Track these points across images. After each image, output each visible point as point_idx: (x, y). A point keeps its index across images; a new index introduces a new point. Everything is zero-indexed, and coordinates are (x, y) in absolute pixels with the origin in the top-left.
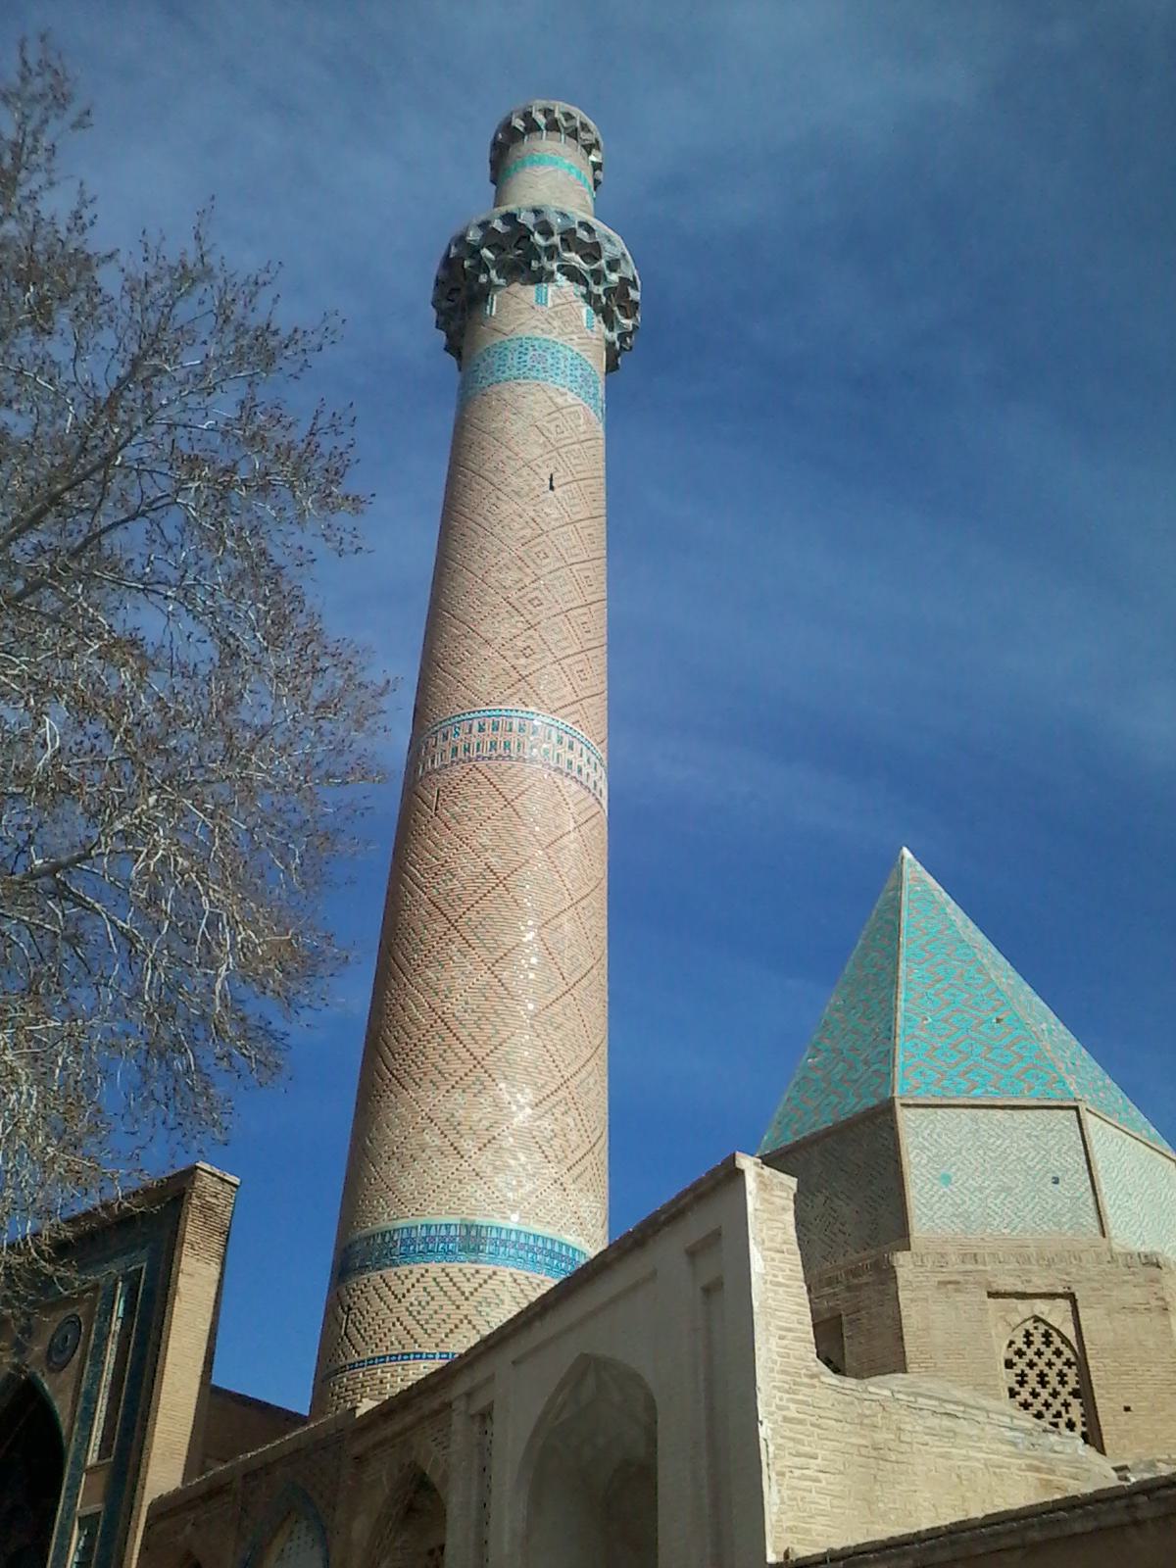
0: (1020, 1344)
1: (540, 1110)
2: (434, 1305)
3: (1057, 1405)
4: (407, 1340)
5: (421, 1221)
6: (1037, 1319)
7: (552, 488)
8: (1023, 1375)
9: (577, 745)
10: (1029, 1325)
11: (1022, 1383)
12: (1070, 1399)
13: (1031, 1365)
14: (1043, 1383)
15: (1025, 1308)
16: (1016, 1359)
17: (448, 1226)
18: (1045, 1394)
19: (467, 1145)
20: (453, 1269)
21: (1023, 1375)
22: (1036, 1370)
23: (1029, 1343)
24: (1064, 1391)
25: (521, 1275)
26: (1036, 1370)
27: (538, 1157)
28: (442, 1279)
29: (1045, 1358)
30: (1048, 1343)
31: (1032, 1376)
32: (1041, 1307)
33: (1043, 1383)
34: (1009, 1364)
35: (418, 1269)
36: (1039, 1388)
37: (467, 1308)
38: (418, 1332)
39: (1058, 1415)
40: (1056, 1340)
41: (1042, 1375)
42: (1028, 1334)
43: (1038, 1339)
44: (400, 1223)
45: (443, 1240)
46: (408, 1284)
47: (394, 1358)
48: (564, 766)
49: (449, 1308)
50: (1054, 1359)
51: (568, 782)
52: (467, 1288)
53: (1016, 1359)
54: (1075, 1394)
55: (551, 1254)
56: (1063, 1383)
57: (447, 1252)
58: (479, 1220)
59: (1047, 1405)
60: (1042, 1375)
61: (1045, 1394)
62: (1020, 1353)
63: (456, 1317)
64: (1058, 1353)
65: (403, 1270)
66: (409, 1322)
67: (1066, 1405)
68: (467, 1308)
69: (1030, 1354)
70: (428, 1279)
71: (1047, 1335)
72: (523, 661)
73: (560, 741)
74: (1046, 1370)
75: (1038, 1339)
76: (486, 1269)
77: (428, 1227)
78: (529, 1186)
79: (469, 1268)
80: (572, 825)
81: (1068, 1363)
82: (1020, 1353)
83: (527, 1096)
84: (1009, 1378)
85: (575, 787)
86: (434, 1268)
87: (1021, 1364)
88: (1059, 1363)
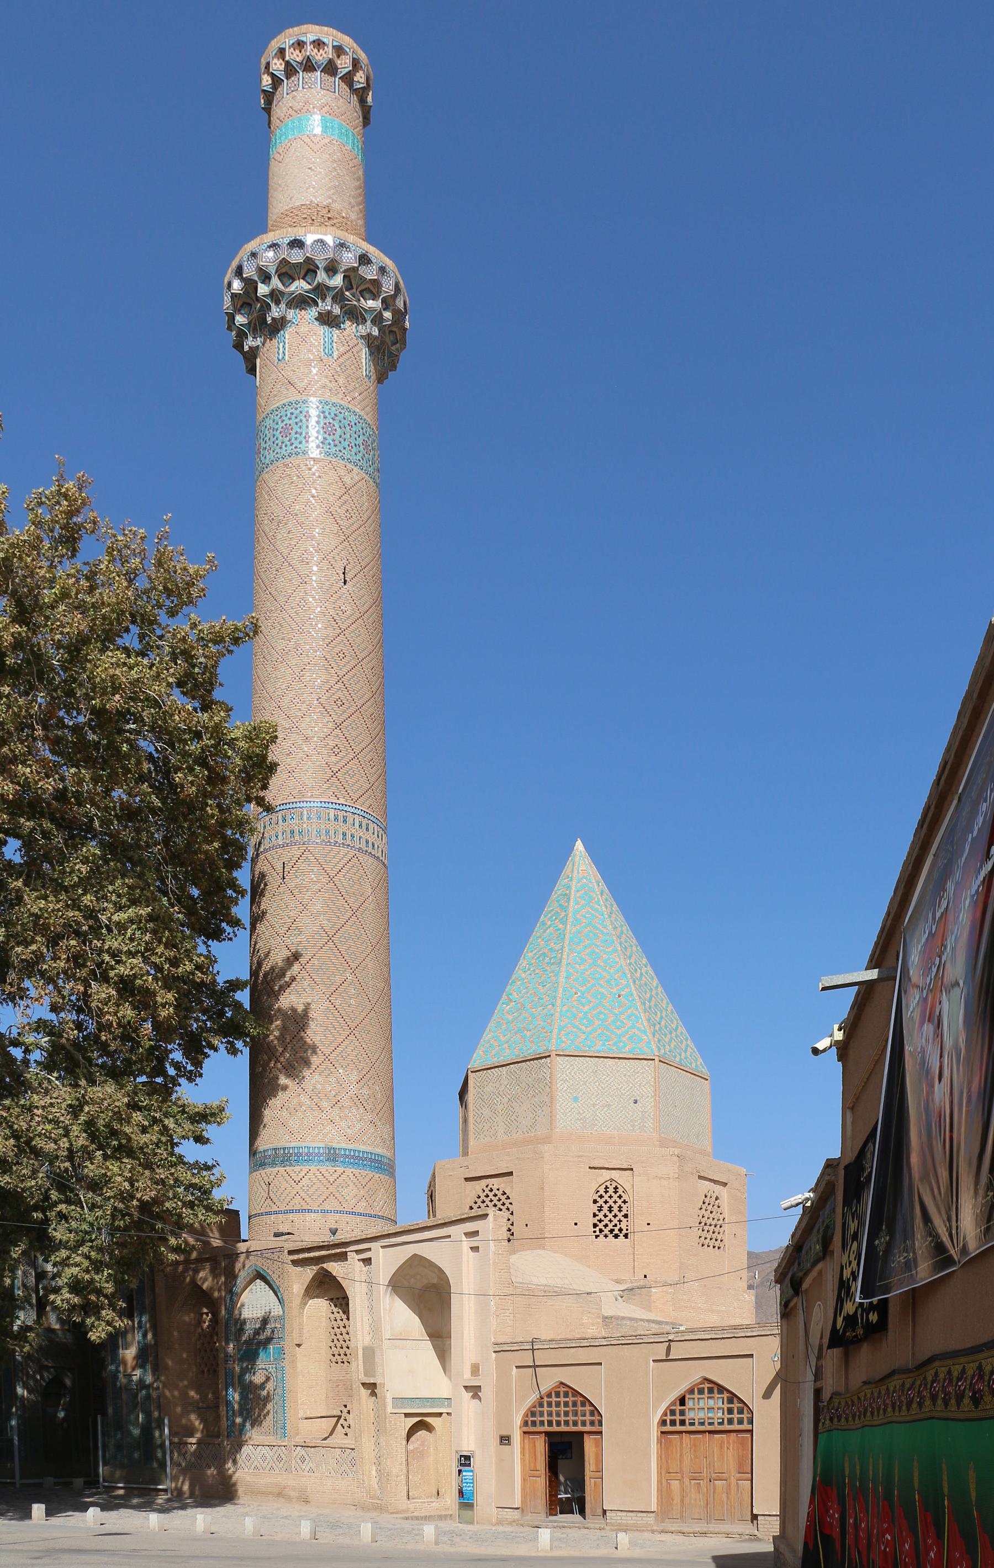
0: (602, 1192)
3: (615, 1221)
4: (303, 1203)
5: (304, 1145)
6: (612, 1180)
7: (345, 582)
8: (601, 1207)
9: (371, 826)
10: (608, 1184)
11: (599, 1211)
12: (622, 1219)
13: (606, 1202)
14: (610, 1211)
15: (606, 1175)
16: (599, 1199)
17: (319, 1148)
18: (610, 1216)
21: (601, 1207)
22: (608, 1205)
23: (606, 1192)
24: (620, 1215)
25: (357, 1172)
26: (608, 1205)
27: (362, 1110)
29: (613, 1199)
30: (616, 1192)
31: (606, 1207)
32: (615, 1175)
33: (610, 1211)
34: (595, 1202)
35: (305, 1169)
36: (608, 1213)
38: (308, 1200)
39: (616, 1225)
40: (620, 1191)
41: (610, 1207)
42: (607, 1187)
43: (611, 1190)
44: (292, 1145)
45: (317, 1155)
46: (301, 1175)
47: (299, 1211)
48: (363, 846)
50: (618, 1200)
51: (367, 857)
52: (332, 1181)
53: (599, 1199)
54: (626, 1216)
55: (371, 1160)
56: (620, 1211)
58: (335, 1145)
59: (611, 1221)
60: (610, 1207)
61: (610, 1216)
62: (601, 1197)
64: (620, 1197)
65: (297, 1168)
67: (620, 1221)
69: (606, 1197)
71: (616, 1188)
72: (333, 759)
73: (360, 826)
74: (613, 1205)
75: (611, 1190)
78: (358, 1126)
79: (332, 1169)
80: (370, 890)
81: (625, 1202)
82: (601, 1197)
83: (354, 1076)
84: (594, 1208)
85: (371, 860)
87: (601, 1202)
88: (620, 1202)
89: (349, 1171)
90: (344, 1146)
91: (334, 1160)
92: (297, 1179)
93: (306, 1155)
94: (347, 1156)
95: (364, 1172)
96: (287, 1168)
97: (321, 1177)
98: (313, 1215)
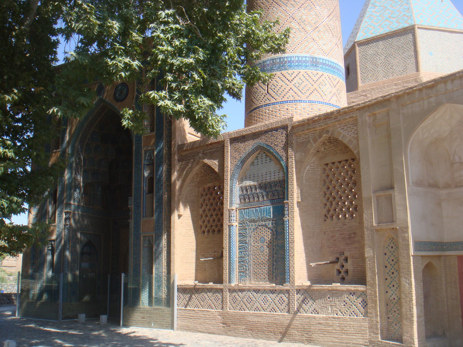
1: (331, 17)
2: (304, 84)
5: (295, 55)
19: (308, 28)
20: (309, 72)
25: (330, 75)
27: (331, 35)
28: (305, 75)
35: (296, 72)
37: (315, 86)
38: (299, 93)
45: (304, 62)
49: (310, 86)
57: (306, 66)
58: (316, 56)
63: (312, 88)
65: (290, 71)
66: (295, 89)
68: (315, 86)
70: (300, 75)
76: (320, 73)
77: (298, 57)
79: (315, 72)
86: (302, 71)
89: (326, 74)
90: (322, 57)
91: (316, 66)
92: (290, 79)
93: (297, 61)
94: (324, 64)
95: (335, 77)
96: (283, 72)
97: (308, 78)
98: (303, 104)
